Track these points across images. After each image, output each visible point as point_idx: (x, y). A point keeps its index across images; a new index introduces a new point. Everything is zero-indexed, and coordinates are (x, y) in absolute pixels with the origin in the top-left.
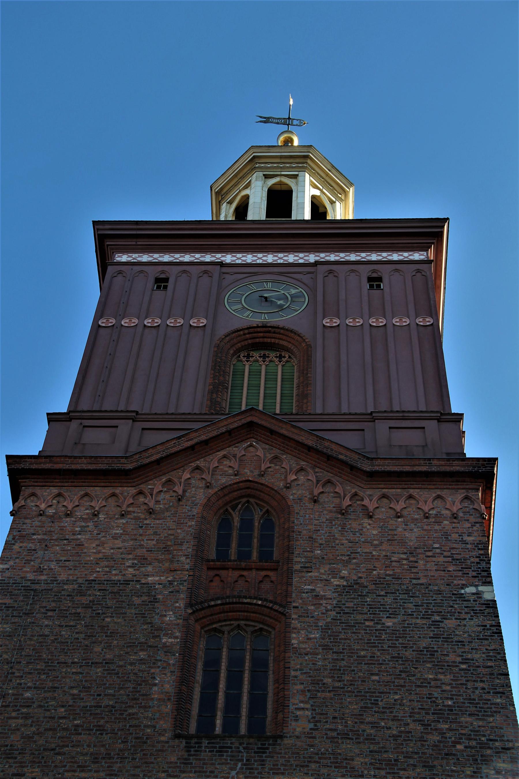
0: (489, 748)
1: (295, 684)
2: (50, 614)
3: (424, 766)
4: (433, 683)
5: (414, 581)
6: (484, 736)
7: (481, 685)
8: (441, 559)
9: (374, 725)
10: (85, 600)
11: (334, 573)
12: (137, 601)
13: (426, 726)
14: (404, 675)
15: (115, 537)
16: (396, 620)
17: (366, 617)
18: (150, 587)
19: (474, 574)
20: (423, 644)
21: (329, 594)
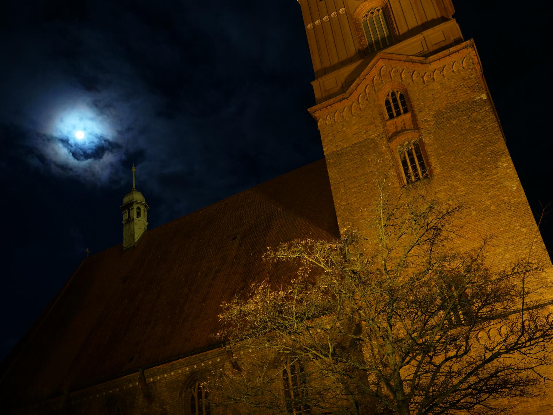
0: (498, 155)
1: (431, 157)
2: (347, 161)
3: (479, 169)
4: (475, 139)
5: (458, 102)
6: (495, 151)
7: (491, 134)
8: (465, 89)
9: (461, 162)
10: (355, 152)
11: (430, 110)
12: (371, 146)
13: (476, 156)
14: (465, 140)
15: (354, 125)
16: (456, 121)
17: (446, 123)
18: (373, 139)
19: (477, 91)
20: (467, 126)
21: (431, 119)
